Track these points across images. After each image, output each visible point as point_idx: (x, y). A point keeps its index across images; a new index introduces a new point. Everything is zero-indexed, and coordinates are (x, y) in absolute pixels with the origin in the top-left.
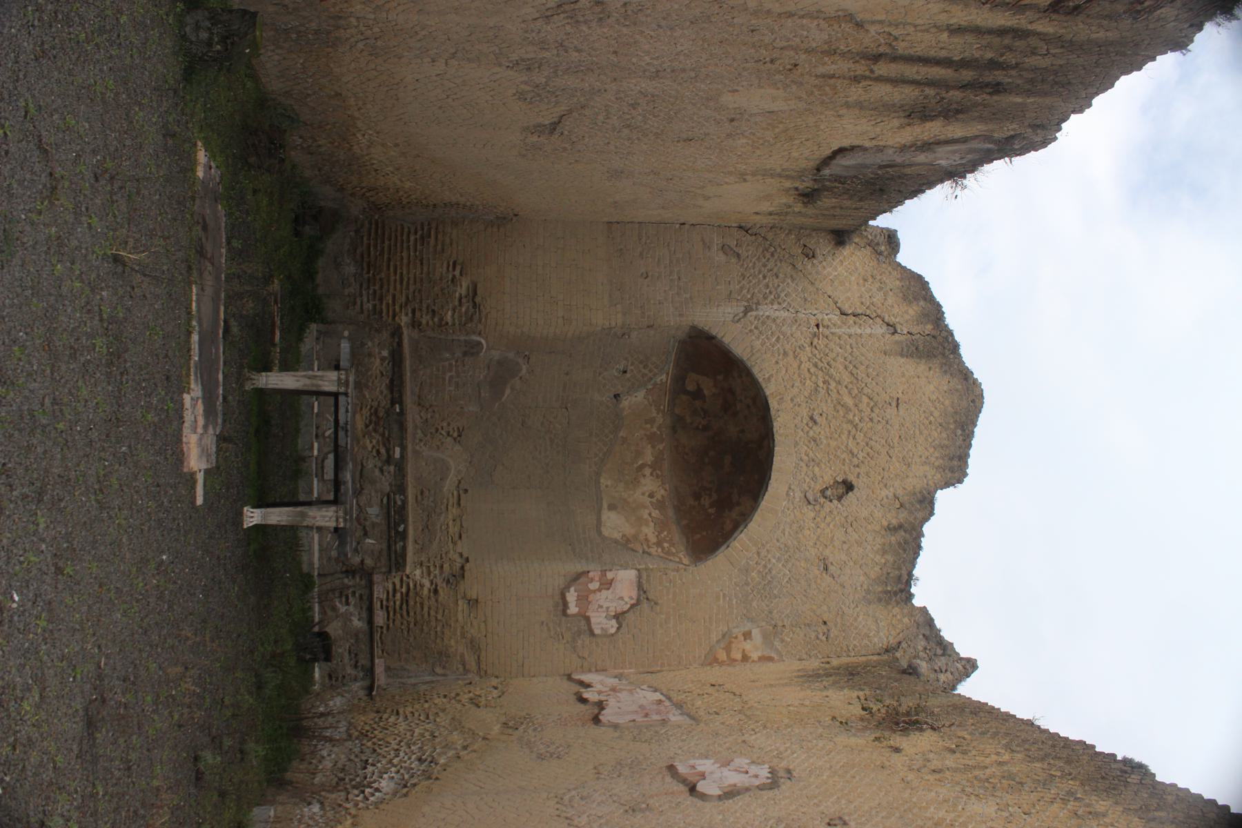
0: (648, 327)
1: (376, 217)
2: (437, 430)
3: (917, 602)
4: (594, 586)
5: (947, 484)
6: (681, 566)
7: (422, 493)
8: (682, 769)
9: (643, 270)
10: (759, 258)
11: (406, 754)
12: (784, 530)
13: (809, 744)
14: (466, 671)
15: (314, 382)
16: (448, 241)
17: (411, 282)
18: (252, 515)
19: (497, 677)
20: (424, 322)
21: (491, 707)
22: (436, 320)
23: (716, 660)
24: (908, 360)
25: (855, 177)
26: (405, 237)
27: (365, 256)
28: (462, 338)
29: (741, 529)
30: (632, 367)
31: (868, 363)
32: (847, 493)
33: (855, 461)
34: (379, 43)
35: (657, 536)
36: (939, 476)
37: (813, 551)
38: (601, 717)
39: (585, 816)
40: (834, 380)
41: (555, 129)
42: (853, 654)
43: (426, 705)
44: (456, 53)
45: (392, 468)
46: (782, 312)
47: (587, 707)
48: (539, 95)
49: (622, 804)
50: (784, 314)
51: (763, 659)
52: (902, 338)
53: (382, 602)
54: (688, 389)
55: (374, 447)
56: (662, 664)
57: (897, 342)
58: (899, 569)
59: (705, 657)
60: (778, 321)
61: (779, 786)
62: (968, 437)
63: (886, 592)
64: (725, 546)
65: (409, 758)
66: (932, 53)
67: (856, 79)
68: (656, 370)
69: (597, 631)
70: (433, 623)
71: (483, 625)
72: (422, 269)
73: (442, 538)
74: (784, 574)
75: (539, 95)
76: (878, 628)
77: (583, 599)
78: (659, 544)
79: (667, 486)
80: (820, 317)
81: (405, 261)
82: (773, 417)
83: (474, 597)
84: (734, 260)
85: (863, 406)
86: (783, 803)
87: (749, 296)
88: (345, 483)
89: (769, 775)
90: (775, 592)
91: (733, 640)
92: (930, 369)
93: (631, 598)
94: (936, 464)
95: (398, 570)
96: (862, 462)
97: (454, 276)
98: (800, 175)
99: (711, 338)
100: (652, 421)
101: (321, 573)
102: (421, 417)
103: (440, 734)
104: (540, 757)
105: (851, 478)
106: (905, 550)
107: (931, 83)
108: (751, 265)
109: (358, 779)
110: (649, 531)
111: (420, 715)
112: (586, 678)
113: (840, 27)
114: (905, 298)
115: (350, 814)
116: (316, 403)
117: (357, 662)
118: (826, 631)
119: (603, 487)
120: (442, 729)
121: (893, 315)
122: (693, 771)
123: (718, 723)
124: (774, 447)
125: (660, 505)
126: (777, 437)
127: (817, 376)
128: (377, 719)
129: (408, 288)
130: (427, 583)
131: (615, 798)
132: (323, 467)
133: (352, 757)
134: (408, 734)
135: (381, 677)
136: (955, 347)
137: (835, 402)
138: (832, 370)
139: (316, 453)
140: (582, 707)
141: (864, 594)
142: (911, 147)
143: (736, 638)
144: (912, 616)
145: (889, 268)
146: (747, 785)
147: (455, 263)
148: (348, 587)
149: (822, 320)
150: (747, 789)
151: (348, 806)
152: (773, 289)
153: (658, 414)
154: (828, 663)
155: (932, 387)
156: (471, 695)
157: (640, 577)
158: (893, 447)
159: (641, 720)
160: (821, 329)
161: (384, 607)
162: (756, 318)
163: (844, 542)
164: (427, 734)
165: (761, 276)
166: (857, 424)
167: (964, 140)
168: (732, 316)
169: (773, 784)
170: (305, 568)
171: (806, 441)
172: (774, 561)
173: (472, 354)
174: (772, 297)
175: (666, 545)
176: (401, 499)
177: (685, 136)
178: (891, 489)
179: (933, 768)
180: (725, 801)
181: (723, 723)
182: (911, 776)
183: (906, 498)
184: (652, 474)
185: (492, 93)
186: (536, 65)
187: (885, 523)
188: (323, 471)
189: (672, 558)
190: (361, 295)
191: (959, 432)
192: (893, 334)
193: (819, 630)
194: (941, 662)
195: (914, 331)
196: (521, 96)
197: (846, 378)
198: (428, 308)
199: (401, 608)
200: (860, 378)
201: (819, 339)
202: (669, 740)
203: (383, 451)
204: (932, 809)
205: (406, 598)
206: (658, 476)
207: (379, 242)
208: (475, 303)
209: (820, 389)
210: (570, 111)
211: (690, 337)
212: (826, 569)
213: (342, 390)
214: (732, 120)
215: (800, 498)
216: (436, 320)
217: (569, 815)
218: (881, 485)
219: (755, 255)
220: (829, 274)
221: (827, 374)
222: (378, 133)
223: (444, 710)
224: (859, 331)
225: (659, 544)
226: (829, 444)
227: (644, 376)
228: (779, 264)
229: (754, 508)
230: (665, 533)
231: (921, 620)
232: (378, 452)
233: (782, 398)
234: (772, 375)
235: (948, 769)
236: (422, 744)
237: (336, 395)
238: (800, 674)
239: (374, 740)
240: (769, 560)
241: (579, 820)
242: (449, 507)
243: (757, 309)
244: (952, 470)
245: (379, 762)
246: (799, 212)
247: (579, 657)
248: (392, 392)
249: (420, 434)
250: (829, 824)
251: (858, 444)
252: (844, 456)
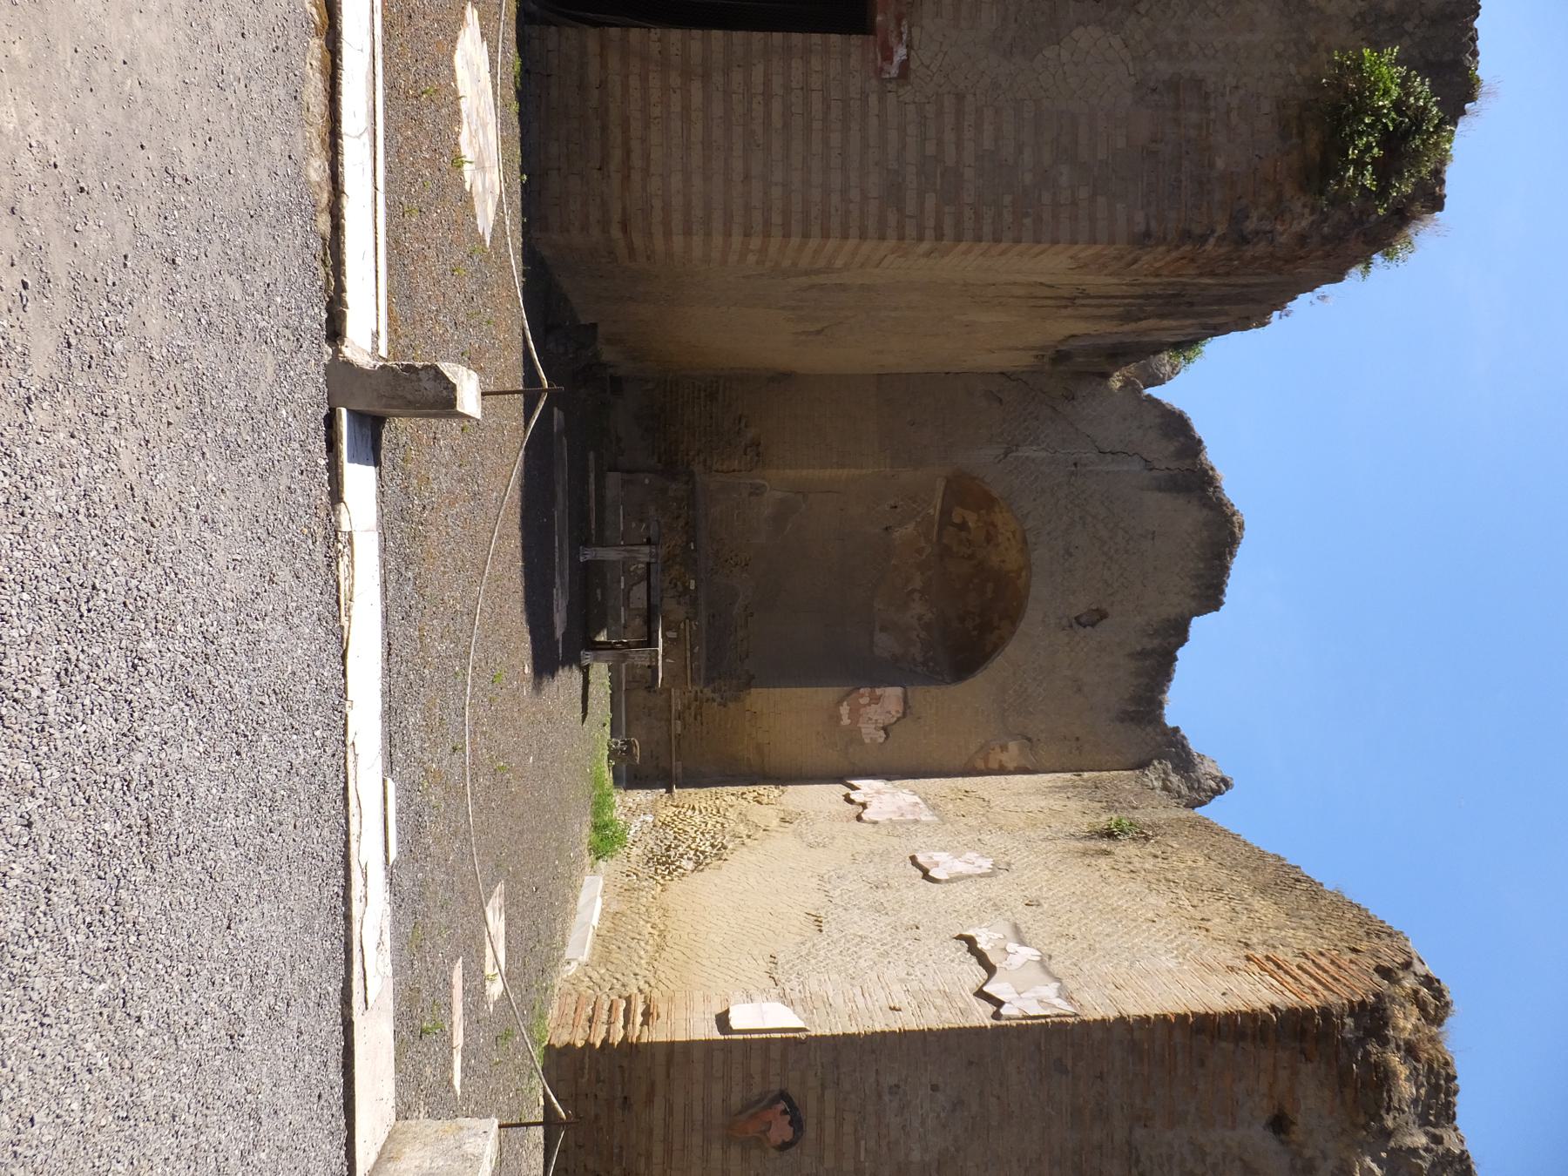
7: (713, 616)
8: (921, 859)
38: (863, 815)
43: (717, 802)
47: (854, 806)
50: (1044, 454)
62: (1223, 571)
69: (867, 741)
77: (855, 712)
79: (934, 610)
93: (897, 712)
94: (1192, 593)
132: (628, 599)
133: (658, 842)
139: (622, 587)
143: (993, 749)
150: (970, 876)
164: (718, 825)
173: (757, 495)
175: (931, 664)
184: (921, 599)
192: (1151, 470)
195: (1171, 467)
212: (1079, 690)
213: (653, 560)
234: (1029, 513)
238: (1050, 785)
242: (738, 628)
243: (1017, 450)
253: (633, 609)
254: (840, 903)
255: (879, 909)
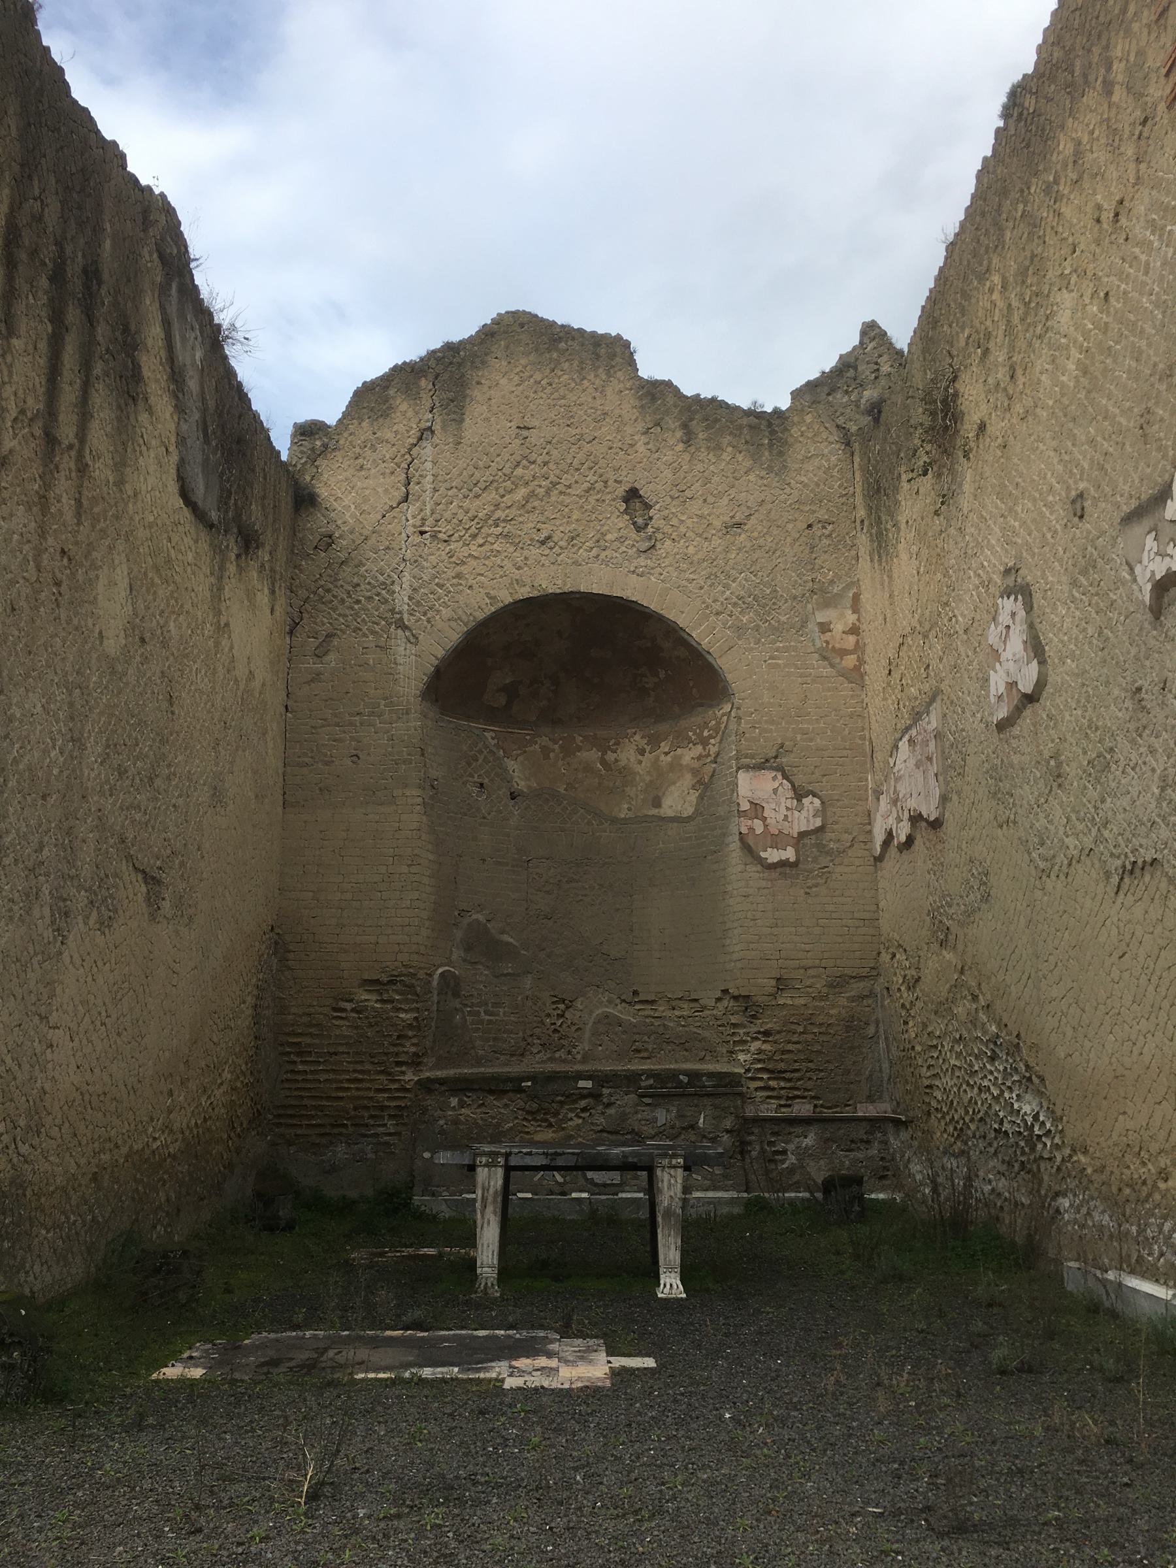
0: (423, 755)
1: (270, 1117)
2: (555, 1031)
3: (785, 403)
4: (759, 829)
5: (632, 363)
6: (733, 714)
7: (638, 1051)
8: (1002, 713)
9: (348, 762)
10: (331, 608)
11: (985, 1076)
12: (688, 580)
13: (972, 544)
14: (872, 994)
15: (490, 1199)
16: (305, 1019)
17: (359, 1067)
18: (668, 1286)
19: (879, 953)
20: (413, 1049)
21: (919, 961)
22: (410, 1033)
23: (857, 668)
24: (467, 413)
25: (221, 477)
26: (300, 1078)
27: (322, 1131)
28: (435, 998)
29: (686, 636)
30: (476, 776)
31: (471, 467)
32: (641, 496)
33: (600, 485)
34: (22, 1122)
35: (694, 745)
36: (619, 374)
37: (716, 542)
38: (932, 819)
39: (1066, 840)
40: (493, 512)
41: (153, 878)
42: (852, 488)
43: (918, 1048)
44: (39, 1015)
45: (605, 1091)
46: (404, 579)
47: (918, 837)
48: (104, 900)
49: (1051, 790)
50: (407, 577)
51: (856, 607)
52: (438, 420)
53: (781, 1106)
54: (504, 703)
55: (578, 1116)
56: (863, 738)
57: (443, 428)
58: (741, 427)
59: (852, 682)
60: (416, 585)
61: (1028, 584)
63: (771, 445)
64: (708, 656)
65: (991, 1073)
66: (42, 362)
67: (83, 469)
68: (480, 745)
69: (818, 822)
70: (809, 1037)
71: (811, 972)
72: (343, 1053)
73: (699, 1024)
74: (746, 580)
75: (104, 900)
76: (817, 456)
77: (777, 840)
78: (705, 742)
80: (410, 530)
81: (332, 1076)
82: (542, 593)
83: (773, 982)
84: (336, 642)
85: (528, 474)
86: (1050, 578)
87: (383, 623)
88: (625, 1156)
89: (1012, 598)
90: (768, 591)
91: (830, 646)
92: (479, 383)
93: (774, 778)
94: (604, 377)
95: (739, 1084)
96: (601, 476)
97: (353, 1010)
98: (219, 551)
99: (438, 674)
100: (546, 751)
101: (744, 1188)
102: (539, 1052)
103: (957, 1030)
104: (986, 898)
105: (621, 490)
106: (716, 421)
107: (86, 365)
108: (341, 620)
109: (1022, 1144)
110: (688, 755)
111: (932, 1057)
112: (879, 837)
113: (6, 488)
114: (385, 415)
115: (1070, 1156)
116: (520, 1195)
117: (862, 1141)
118: (820, 525)
119: (630, 814)
120: (951, 1028)
121: (408, 431)
122: (1005, 698)
123: (941, 666)
124: (580, 592)
125: (655, 741)
126: (567, 588)
127: (489, 535)
128: (939, 1116)
129: (368, 1072)
130: (756, 1045)
131: (1042, 800)
132: (605, 1185)
133: (992, 1150)
134: (957, 1074)
135: (882, 1108)
136: (450, 348)
137: (522, 512)
138: (480, 515)
139: (585, 1195)
140: (918, 842)
141: (772, 475)
142: (177, 398)
144: (802, 410)
145: (346, 435)
146: (1025, 627)
147: (335, 1010)
148: (763, 1151)
149: (414, 526)
150: (1031, 626)
151: (1059, 1159)
152: (374, 591)
153: (536, 743)
154: (862, 522)
155: (503, 381)
156: (903, 988)
157: (747, 768)
158: (582, 435)
159: (935, 765)
160: (427, 529)
161: (790, 1102)
162: (411, 614)
163: (705, 500)
164: (957, 1049)
165: (356, 607)
166: (551, 483)
167: (167, 324)
168: (409, 645)
169: (1024, 592)
170: (736, 1210)
171: (574, 550)
172: (728, 593)
174: (384, 592)
175: (706, 733)
176: (646, 1079)
177: (165, 705)
178: (636, 438)
179: (1008, 378)
180: (1047, 655)
181: (941, 659)
182: (1018, 408)
183: (648, 418)
185: (100, 963)
186: (61, 904)
187: (681, 447)
188: (609, 1185)
189: (723, 726)
190: (376, 1135)
191: (562, 345)
192: (433, 432)
193: (819, 533)
194: (865, 371)
195: (429, 405)
196: (104, 925)
197: (491, 496)
198: (395, 1045)
199: (790, 1080)
200: (492, 478)
201: (440, 532)
202: (963, 730)
203: (583, 1103)
204: (1064, 379)
205: (776, 1074)
206: (617, 743)
207: (304, 1112)
208: (390, 982)
209: (506, 530)
210: (129, 857)
211: (437, 701)
212: (739, 525)
213: (501, 1160)
214: (143, 640)
215: (646, 558)
216: (410, 1033)
217: (1066, 862)
218: (630, 451)
219: (329, 613)
220: (353, 516)
221: (486, 521)
222: (152, 1119)
223: (925, 1026)
224: (429, 478)
225: (705, 742)
226: (577, 520)
227: (485, 759)
228: (341, 582)
229: (660, 619)
230: (690, 734)
231: (808, 397)
232: (584, 1110)
233: (517, 580)
234: (487, 594)
235: (1010, 358)
236: (970, 1055)
237: (508, 1169)
239: (967, 1119)
240: (726, 599)
241: (1071, 847)
243: (400, 613)
244: (612, 356)
245: (997, 1115)
246: (270, 554)
247: (852, 846)
248: (504, 1092)
249: (561, 1054)
250: (1081, 517)
251: (576, 482)
252: (592, 500)
253: (621, 1180)
254: (1094, 831)
255: (1100, 766)
